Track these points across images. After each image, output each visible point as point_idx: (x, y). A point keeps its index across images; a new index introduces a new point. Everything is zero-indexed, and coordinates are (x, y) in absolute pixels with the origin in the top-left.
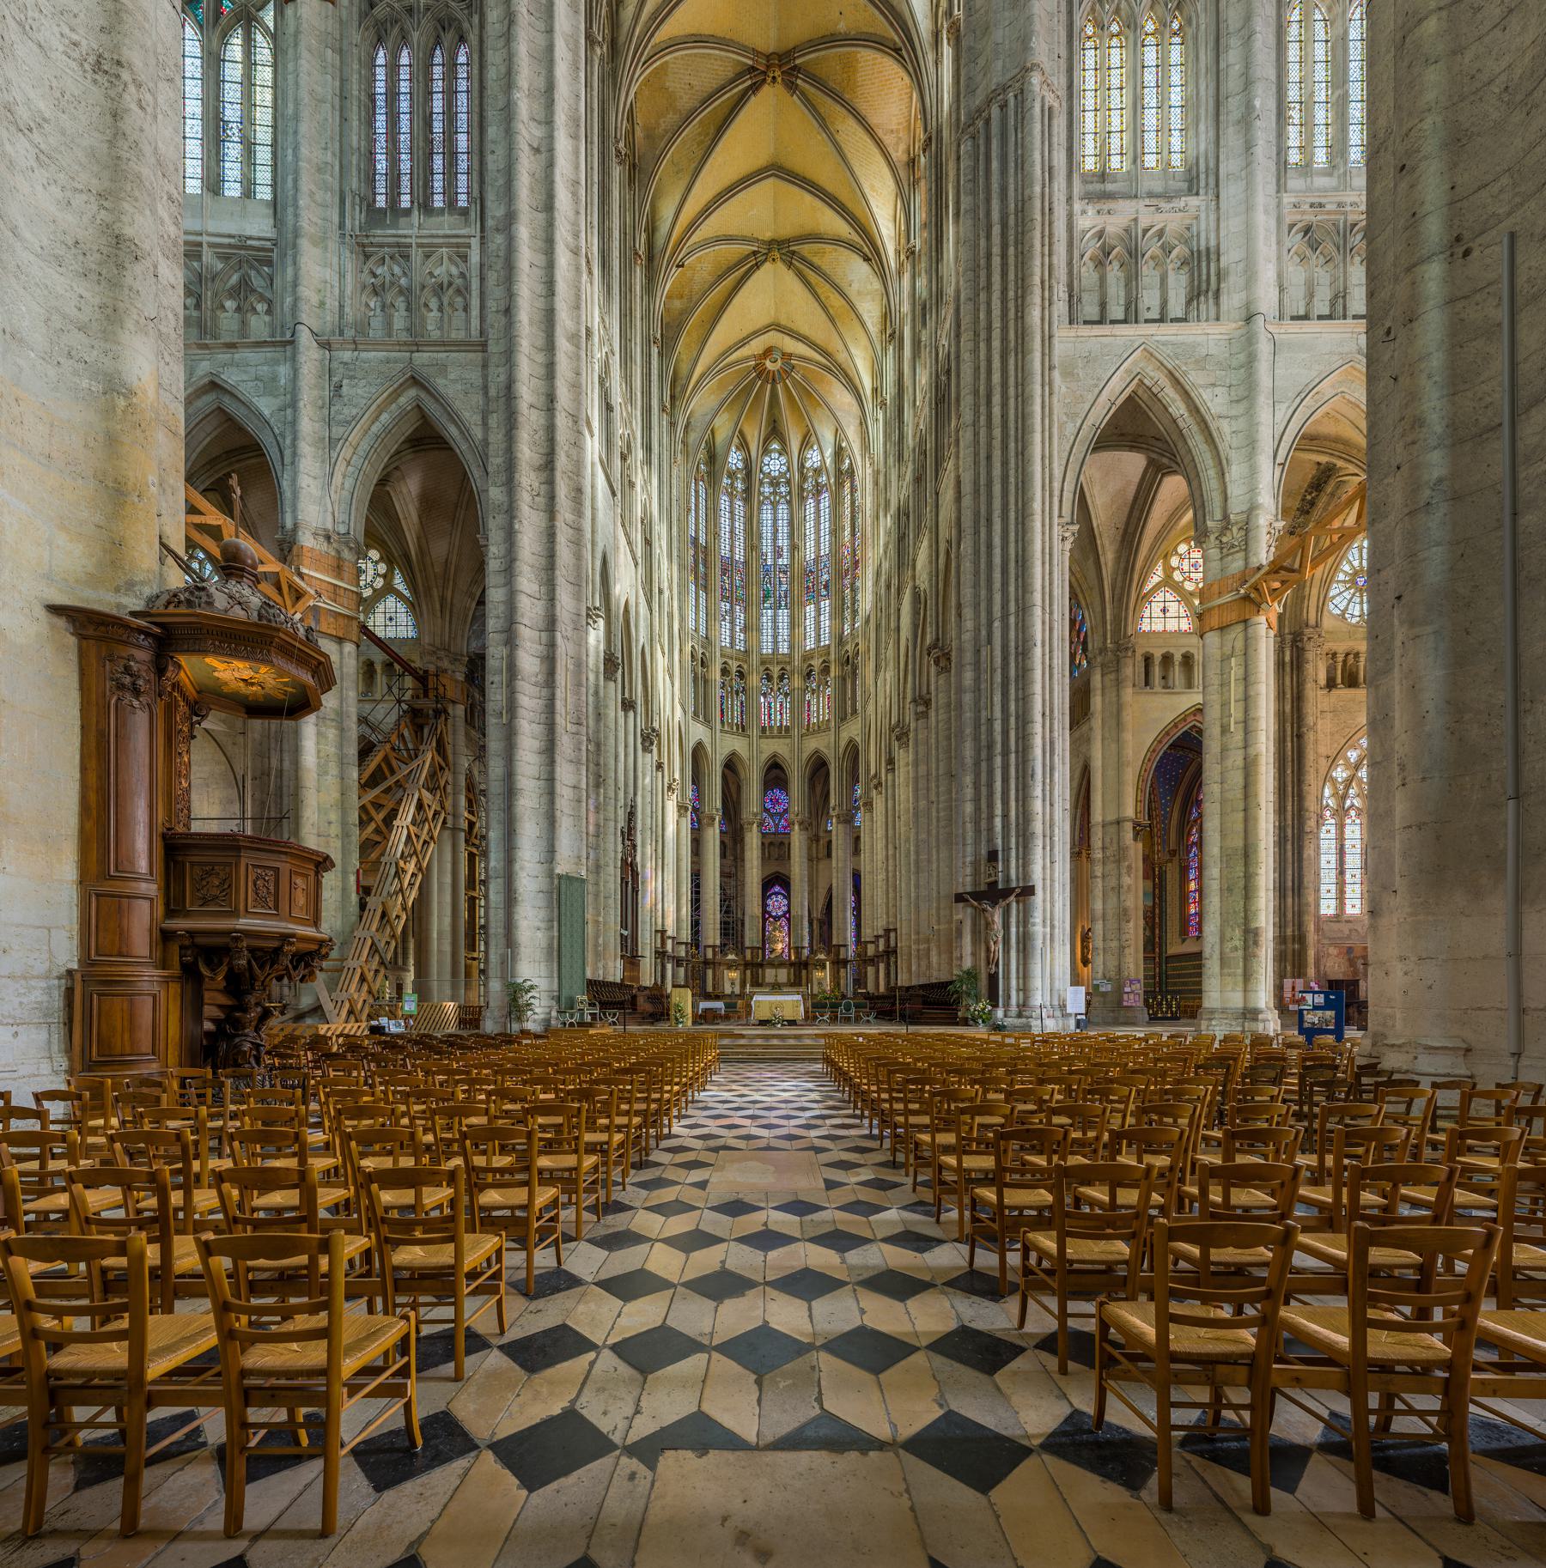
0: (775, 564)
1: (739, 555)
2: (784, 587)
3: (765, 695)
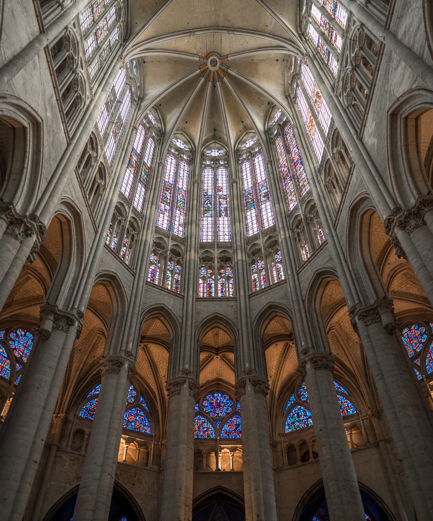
0: (215, 195)
1: (183, 184)
3: (204, 279)
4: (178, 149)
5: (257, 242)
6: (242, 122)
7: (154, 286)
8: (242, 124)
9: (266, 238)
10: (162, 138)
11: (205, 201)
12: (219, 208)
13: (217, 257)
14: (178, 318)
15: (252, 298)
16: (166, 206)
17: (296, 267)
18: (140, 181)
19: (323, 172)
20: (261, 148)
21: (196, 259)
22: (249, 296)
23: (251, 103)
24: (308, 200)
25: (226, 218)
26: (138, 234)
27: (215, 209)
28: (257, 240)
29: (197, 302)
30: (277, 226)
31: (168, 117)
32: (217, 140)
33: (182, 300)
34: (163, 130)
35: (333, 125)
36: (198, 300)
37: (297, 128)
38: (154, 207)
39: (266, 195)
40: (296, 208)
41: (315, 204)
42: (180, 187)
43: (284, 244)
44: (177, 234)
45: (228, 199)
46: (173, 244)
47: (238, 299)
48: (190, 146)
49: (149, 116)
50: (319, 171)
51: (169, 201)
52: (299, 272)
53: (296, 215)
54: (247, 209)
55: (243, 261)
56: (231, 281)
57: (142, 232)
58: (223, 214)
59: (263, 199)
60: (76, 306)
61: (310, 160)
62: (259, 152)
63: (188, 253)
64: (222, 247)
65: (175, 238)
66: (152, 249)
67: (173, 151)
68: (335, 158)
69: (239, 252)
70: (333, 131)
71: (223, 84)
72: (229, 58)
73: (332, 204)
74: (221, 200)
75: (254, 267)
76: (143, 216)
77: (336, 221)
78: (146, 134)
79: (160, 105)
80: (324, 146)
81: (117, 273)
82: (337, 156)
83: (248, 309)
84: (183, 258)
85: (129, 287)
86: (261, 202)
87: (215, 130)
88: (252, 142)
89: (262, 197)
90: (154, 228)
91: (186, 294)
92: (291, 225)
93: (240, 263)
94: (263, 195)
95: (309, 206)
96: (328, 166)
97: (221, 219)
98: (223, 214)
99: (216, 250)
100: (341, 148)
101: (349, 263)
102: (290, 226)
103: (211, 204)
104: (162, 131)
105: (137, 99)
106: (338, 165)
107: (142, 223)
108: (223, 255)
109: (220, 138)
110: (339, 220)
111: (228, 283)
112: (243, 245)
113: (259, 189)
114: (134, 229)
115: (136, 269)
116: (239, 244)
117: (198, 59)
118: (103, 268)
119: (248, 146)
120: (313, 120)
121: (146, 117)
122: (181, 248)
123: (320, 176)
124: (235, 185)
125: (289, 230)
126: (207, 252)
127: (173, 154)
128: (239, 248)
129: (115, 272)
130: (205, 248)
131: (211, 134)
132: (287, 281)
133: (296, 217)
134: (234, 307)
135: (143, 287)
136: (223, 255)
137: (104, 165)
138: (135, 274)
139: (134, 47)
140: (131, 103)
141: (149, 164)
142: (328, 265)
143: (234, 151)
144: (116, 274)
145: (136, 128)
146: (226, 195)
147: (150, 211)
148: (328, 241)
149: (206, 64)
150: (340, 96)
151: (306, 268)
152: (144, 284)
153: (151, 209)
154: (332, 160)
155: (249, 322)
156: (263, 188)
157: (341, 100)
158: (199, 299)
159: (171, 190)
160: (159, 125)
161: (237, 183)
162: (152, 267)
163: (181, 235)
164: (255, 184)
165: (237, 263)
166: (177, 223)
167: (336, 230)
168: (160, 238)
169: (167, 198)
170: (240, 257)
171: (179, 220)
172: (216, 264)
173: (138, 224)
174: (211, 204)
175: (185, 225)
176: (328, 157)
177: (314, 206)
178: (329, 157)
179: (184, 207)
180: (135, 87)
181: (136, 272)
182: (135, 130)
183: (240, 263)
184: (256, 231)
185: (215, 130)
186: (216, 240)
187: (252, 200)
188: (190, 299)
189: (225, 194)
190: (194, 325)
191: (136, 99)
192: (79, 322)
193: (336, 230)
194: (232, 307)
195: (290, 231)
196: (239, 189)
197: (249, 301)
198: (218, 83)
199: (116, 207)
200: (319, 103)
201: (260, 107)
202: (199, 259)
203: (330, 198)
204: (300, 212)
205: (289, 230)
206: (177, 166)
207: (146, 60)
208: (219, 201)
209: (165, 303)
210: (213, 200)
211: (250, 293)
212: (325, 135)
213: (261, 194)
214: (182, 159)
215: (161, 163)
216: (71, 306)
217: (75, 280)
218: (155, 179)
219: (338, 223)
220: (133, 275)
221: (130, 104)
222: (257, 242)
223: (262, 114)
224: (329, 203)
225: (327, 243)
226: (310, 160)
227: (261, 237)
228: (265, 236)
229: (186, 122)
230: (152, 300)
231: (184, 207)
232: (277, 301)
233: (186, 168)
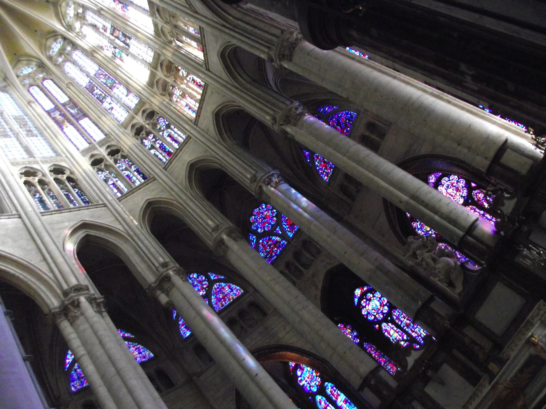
18: (78, 120)
31: (28, 50)
34: (40, 62)
38: (103, 118)
51: (103, 95)
60: (157, 265)
63: (153, 104)
64: (157, 64)
67: (60, 60)
69: (164, 51)
74: (115, 34)
105: (5, 84)
108: (164, 67)
115: (150, 174)
118: (137, 213)
126: (157, 82)
129: (145, 200)
131: (51, 8)
135: (167, 176)
136: (164, 67)
138: (154, 177)
144: (147, 200)
152: (165, 172)
155: (229, 86)
158: (196, 122)
161: (102, 9)
173: (114, 145)
192: (170, 269)
206: (74, 63)
209: (190, 159)
216: (154, 269)
217: (137, 252)
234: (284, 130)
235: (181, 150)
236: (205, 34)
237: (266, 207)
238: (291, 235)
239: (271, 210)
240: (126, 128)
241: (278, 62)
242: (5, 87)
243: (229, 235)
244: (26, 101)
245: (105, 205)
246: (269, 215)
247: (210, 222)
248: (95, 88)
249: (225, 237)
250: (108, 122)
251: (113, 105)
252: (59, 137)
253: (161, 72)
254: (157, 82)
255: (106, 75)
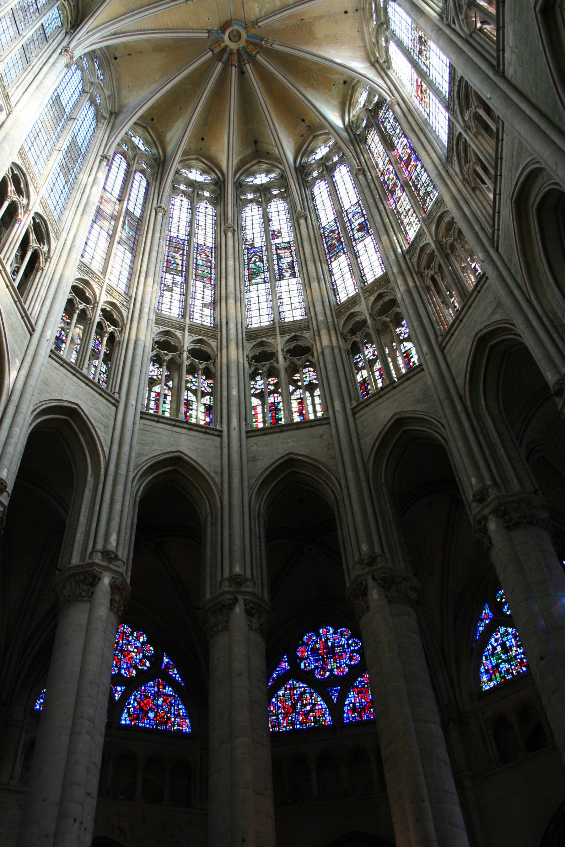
0: (268, 245)
2: (286, 261)
4: (191, 184)
5: (356, 309)
6: (303, 120)
7: (158, 418)
8: (303, 123)
9: (372, 298)
10: (160, 169)
11: (251, 258)
12: (278, 264)
13: (283, 350)
14: (213, 475)
15: (361, 413)
16: (175, 276)
17: (437, 336)
19: (455, 158)
20: (343, 154)
21: (241, 360)
22: (352, 409)
23: (313, 86)
24: (439, 214)
25: (293, 281)
26: (121, 332)
27: (270, 268)
28: (356, 305)
29: (250, 439)
30: (390, 273)
31: (169, 136)
32: (263, 158)
33: (219, 439)
34: (162, 158)
35: (454, 74)
36: (249, 435)
37: (399, 104)
38: (150, 280)
39: (362, 227)
40: (419, 235)
41: (453, 218)
42: (201, 242)
43: (407, 301)
44: (200, 322)
45: (293, 248)
46: (192, 339)
47: (332, 419)
48: (214, 176)
49: (133, 139)
50: (449, 159)
52: (443, 345)
53: (421, 245)
54: (330, 258)
55: (332, 349)
56: (317, 392)
57: (128, 326)
58: (287, 274)
59: (358, 235)
61: (429, 148)
62: (341, 161)
65: (195, 329)
66: (150, 353)
67: (183, 187)
68: (469, 128)
69: (324, 332)
70: (457, 84)
71: (258, 66)
72: (259, 24)
73: (482, 209)
74: (279, 252)
75: (360, 357)
76: (131, 297)
77: (493, 232)
78: (129, 166)
79: (152, 120)
80: (447, 115)
81: (79, 402)
82: (473, 124)
83: (354, 435)
84: (215, 362)
85: (106, 427)
86: (355, 240)
87: (256, 142)
88: (327, 149)
89: (355, 232)
90: (153, 317)
91: (225, 428)
92: (416, 266)
93: (327, 352)
94: (358, 227)
95: (443, 225)
96: (461, 147)
97: (283, 283)
98: (287, 274)
99: (279, 338)
100: (475, 108)
101: (535, 303)
102: (413, 267)
103: (262, 260)
104: (160, 158)
105: (107, 115)
106: (477, 138)
107: (129, 310)
109: (268, 153)
110: (498, 230)
111: (312, 396)
112: (330, 320)
113: (349, 220)
114: (114, 323)
115: (119, 393)
116: (321, 318)
117: (207, 35)
119: (318, 156)
120: (423, 84)
121: (127, 140)
122: (209, 345)
123: (452, 167)
124: (302, 221)
125: (414, 274)
127: (184, 192)
128: (321, 326)
129: (75, 401)
130: (258, 338)
131: (250, 151)
132: (424, 367)
133: (422, 249)
134: (325, 436)
135: (134, 423)
136: (293, 344)
137: (45, 217)
138: (118, 402)
139: (90, 34)
140: (97, 121)
141: (138, 213)
142: (497, 317)
143: (295, 168)
145: (106, 158)
146: (289, 243)
147: (144, 288)
148: (487, 275)
149: (219, 41)
150: (454, 23)
151: (456, 334)
152: (138, 418)
153: (145, 284)
154: (466, 131)
155: (358, 459)
156: (356, 217)
157: (457, 28)
158: (252, 433)
159: (184, 250)
160: (154, 151)
162: (157, 389)
163: (207, 322)
164: (340, 212)
165: (323, 353)
166: (198, 303)
167: (497, 250)
168: (167, 333)
169: (177, 264)
170: (325, 342)
171: (203, 298)
172: (282, 362)
173: (120, 313)
174: (262, 260)
175: (214, 304)
176: (458, 131)
177: (452, 223)
178: (460, 130)
179: (211, 274)
180: (102, 97)
181: (119, 397)
182: (105, 160)
183: (327, 352)
184: (352, 292)
185: (256, 142)
186: (277, 321)
187: (339, 240)
188: (235, 434)
189: (287, 240)
190: (245, 484)
191: (105, 114)
193: (497, 250)
194: (321, 436)
195: (415, 277)
196: (310, 227)
197: (355, 420)
198: (247, 65)
199: (75, 289)
200: (425, 53)
201: (330, 90)
202: (246, 359)
203: (476, 199)
204: (428, 239)
205: (414, 274)
206: (193, 209)
207: (118, 55)
208: (277, 254)
210: (265, 253)
211: (355, 403)
212: (444, 97)
213: (353, 227)
214: (201, 198)
215: (160, 207)
218: (150, 235)
219: (498, 236)
220: (114, 405)
221: (94, 123)
222: (356, 309)
223: (335, 102)
224: (476, 207)
225: (487, 278)
226: (429, 148)
227: (363, 299)
228: (370, 296)
229: (203, 139)
230: (155, 447)
231: (211, 274)
232: (410, 409)
233: (210, 210)
234: (367, 587)
235: (190, 429)
236: (414, 379)
237: (143, 643)
238: (125, 720)
239: (144, 656)
240: (157, 322)
241: (486, 511)
242: (104, 118)
243: (114, 587)
244: (103, 152)
245: (31, 330)
246: (132, 657)
247: (113, 538)
248: (181, 253)
249: (106, 580)
250: (149, 289)
251: (177, 290)
252: (85, 216)
253: (283, 343)
254: (262, 344)
255: (211, 262)
